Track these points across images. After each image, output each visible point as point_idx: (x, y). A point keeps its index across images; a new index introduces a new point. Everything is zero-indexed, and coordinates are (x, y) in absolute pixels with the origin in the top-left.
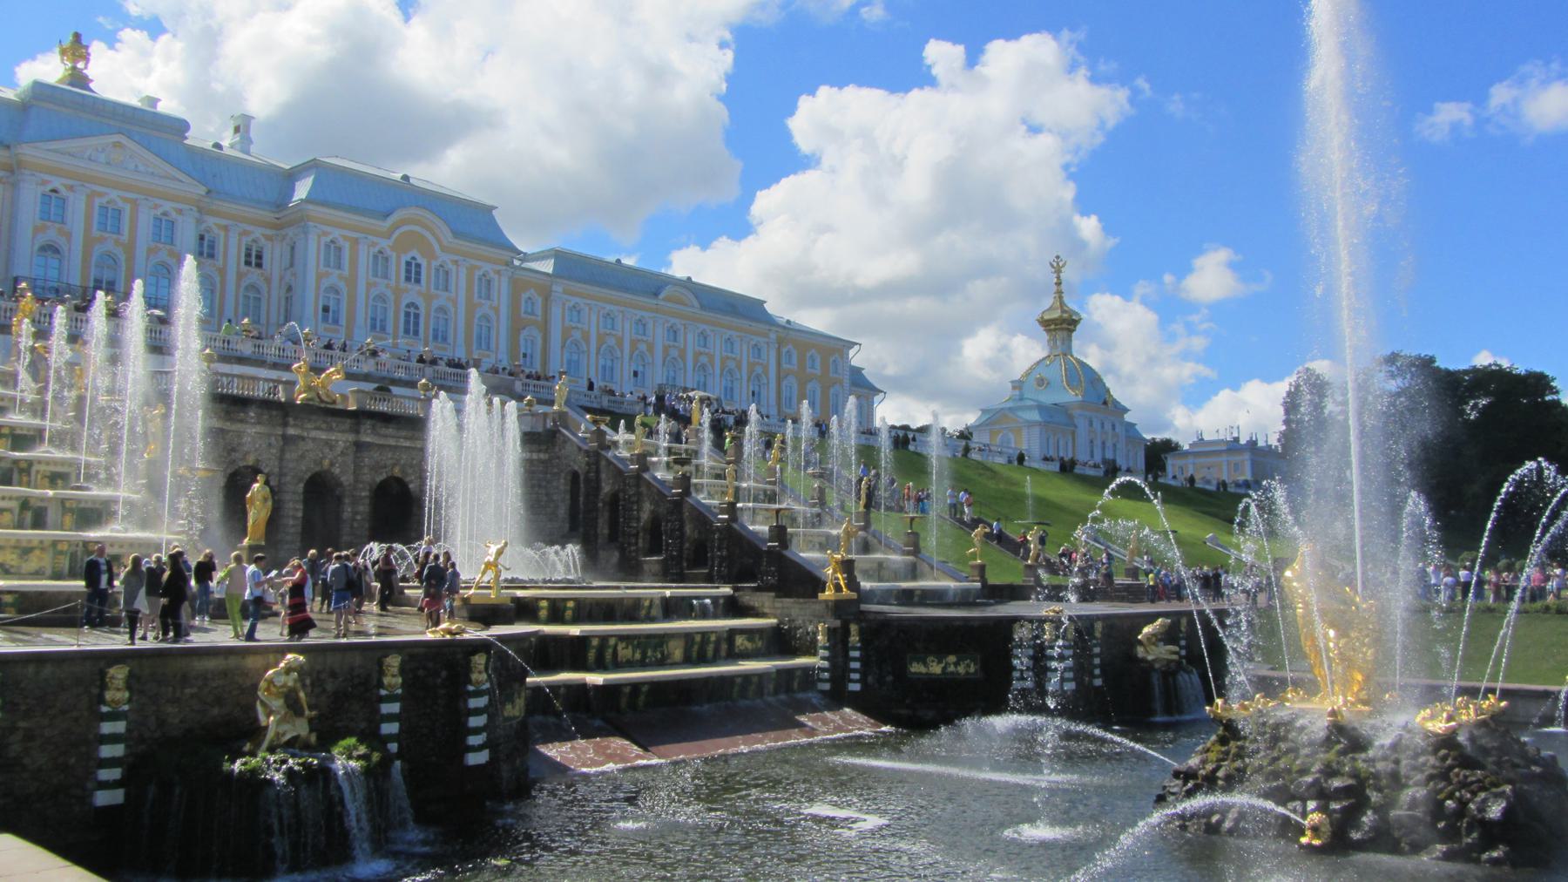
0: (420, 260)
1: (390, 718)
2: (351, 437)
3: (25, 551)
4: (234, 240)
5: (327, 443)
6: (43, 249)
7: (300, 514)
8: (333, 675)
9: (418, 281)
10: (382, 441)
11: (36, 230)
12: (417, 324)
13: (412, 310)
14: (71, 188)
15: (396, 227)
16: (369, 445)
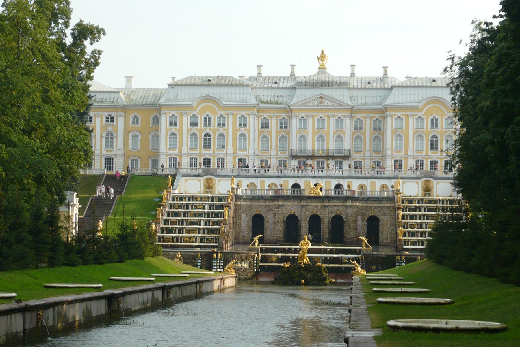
0: (437, 117)
1: (199, 263)
2: (322, 204)
3: (190, 238)
4: (368, 122)
5: (315, 206)
6: (300, 137)
7: (307, 227)
8: (191, 255)
9: (437, 126)
10: (333, 204)
11: (298, 132)
12: (437, 145)
13: (434, 139)
14: (307, 116)
15: (424, 107)
16: (327, 206)
